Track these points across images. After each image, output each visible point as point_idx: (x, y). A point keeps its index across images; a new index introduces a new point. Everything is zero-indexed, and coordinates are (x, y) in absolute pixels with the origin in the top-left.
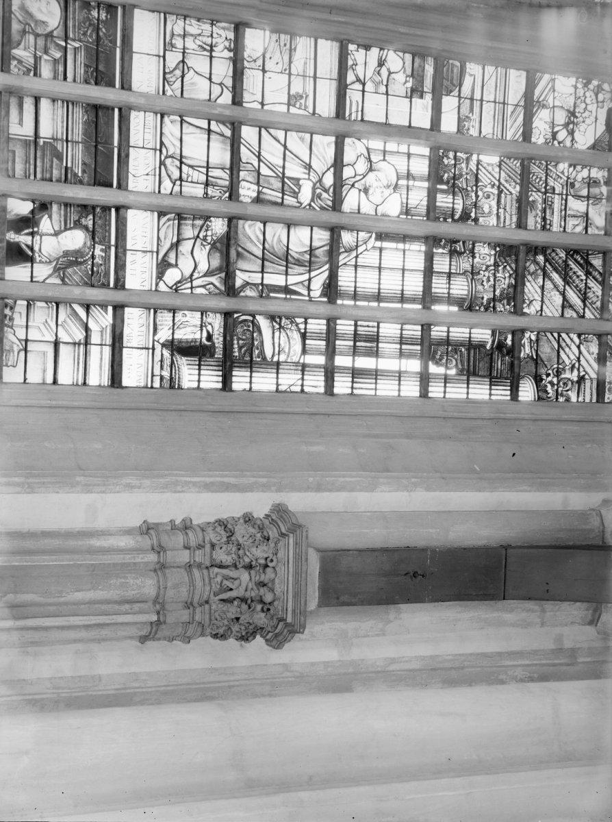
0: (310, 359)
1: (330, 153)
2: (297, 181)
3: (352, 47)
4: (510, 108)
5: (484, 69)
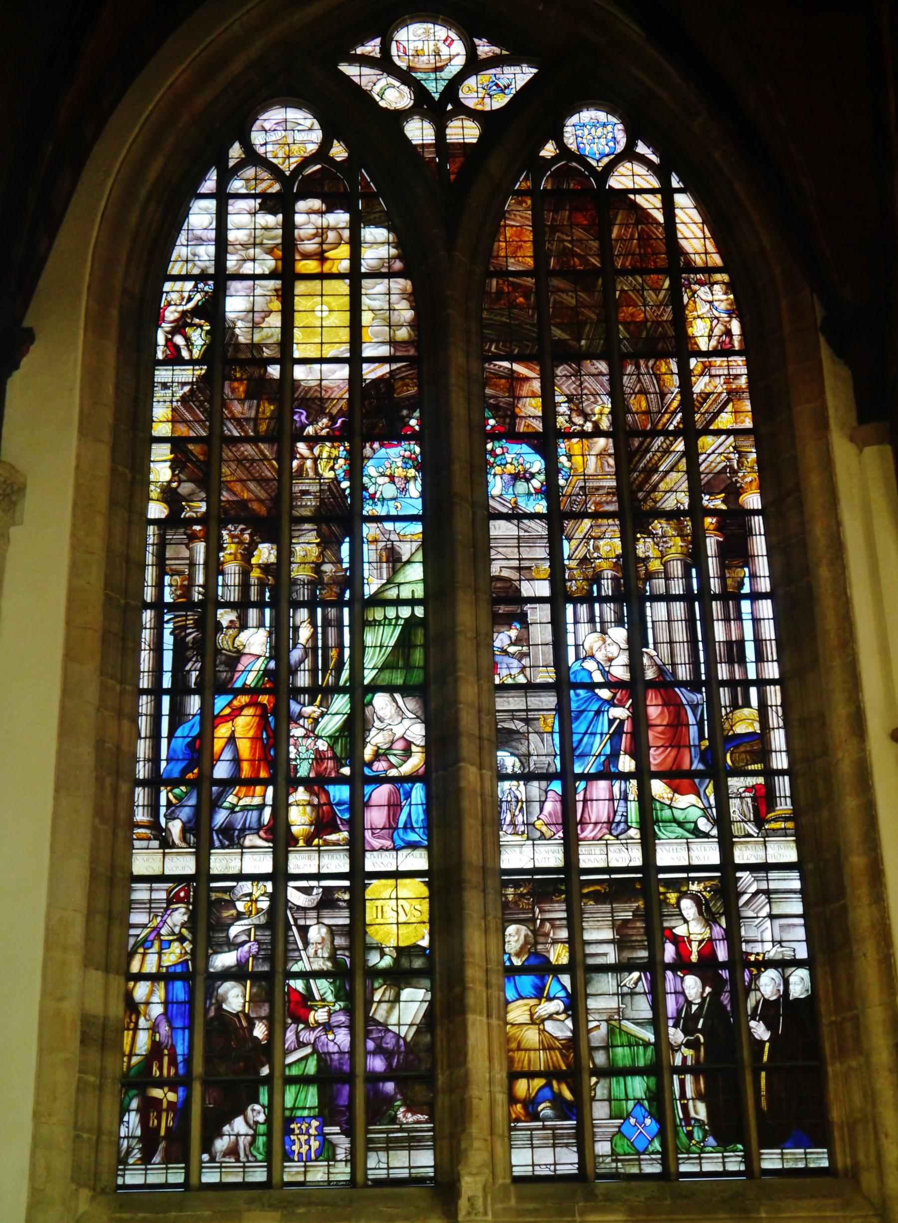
0: (754, 701)
1: (582, 692)
2: (611, 722)
3: (497, 681)
4: (522, 533)
5: (494, 560)
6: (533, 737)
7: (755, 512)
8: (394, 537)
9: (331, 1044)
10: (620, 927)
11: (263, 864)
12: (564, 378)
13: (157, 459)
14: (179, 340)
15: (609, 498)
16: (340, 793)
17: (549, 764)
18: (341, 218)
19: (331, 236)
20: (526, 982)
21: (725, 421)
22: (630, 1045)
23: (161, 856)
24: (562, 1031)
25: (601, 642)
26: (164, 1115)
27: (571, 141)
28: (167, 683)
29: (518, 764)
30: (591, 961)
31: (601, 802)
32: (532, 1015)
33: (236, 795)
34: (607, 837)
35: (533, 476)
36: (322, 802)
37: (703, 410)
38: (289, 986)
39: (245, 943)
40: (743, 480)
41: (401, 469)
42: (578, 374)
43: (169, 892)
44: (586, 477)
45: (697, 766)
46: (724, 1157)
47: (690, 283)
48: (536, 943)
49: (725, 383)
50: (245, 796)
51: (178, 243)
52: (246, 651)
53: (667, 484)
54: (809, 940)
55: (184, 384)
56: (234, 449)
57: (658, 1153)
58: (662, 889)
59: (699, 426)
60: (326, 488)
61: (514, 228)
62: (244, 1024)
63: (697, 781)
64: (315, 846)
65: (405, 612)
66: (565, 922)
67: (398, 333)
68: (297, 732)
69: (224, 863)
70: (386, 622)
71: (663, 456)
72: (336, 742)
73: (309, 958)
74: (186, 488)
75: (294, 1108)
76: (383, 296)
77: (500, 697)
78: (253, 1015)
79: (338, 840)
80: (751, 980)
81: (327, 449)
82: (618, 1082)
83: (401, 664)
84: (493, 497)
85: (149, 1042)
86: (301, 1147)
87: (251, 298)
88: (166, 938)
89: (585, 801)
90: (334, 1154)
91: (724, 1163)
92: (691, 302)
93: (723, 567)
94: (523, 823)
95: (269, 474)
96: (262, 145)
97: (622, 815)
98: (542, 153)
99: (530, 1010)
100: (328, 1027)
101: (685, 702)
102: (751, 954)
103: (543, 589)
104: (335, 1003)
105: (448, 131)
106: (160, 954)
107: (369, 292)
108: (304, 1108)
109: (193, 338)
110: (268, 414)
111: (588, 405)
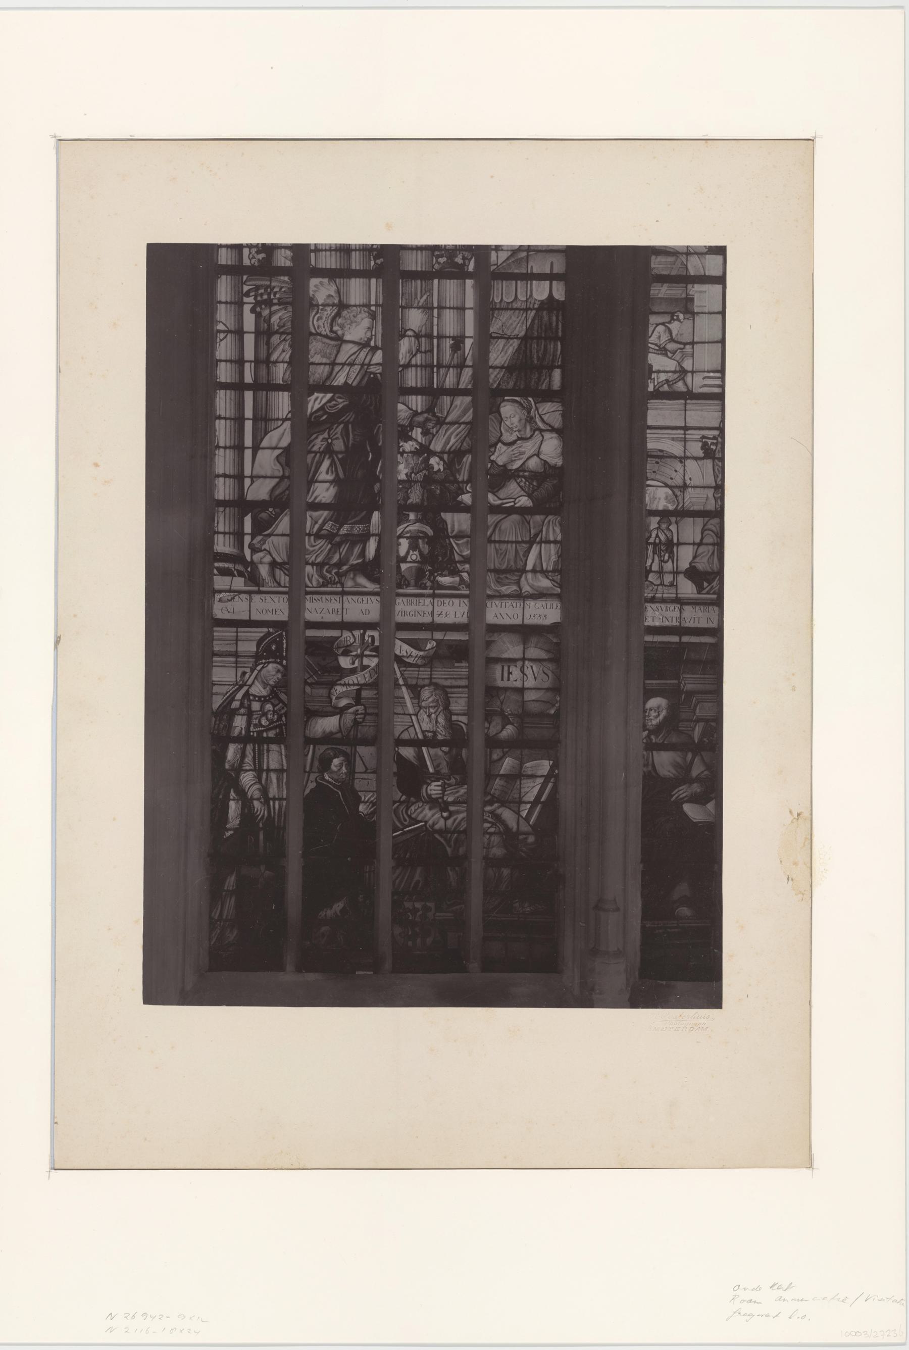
17: (707, 498)
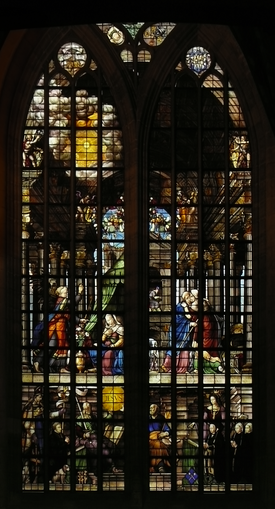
2: (190, 328)
6: (162, 333)
7: (250, 242)
8: (113, 249)
9: (91, 445)
10: (189, 406)
11: (67, 380)
12: (180, 179)
13: (24, 212)
14: (31, 158)
15: (195, 234)
16: (94, 353)
18: (93, 100)
19: (90, 108)
20: (156, 425)
21: (241, 200)
22: (190, 448)
23: (32, 376)
24: (168, 442)
25: (188, 295)
26: (36, 468)
27: (189, 62)
28: (31, 309)
29: (156, 344)
30: (179, 418)
31: (185, 359)
32: (158, 437)
33: (57, 353)
34: (187, 372)
35: (167, 223)
36: (87, 356)
37: (233, 195)
38: (77, 424)
39: (61, 408)
40: (246, 227)
41: (116, 219)
42: (185, 177)
43: (35, 389)
44: (187, 224)
45: (220, 346)
46: (218, 486)
47: (232, 135)
48: (160, 411)
49: (242, 183)
50: (61, 354)
51: (29, 111)
52: (60, 296)
53: (217, 228)
54: (253, 413)
55: (33, 178)
56: (54, 209)
57: (197, 484)
58: (204, 393)
59: (231, 203)
60: (88, 227)
61: (164, 106)
62: (62, 437)
63: (219, 352)
64: (85, 373)
65: (117, 281)
66: (170, 404)
67: (117, 156)
68: (79, 329)
69: (54, 379)
70: (110, 285)
71: (216, 216)
72: (92, 333)
73: (83, 414)
74: (36, 226)
75: (79, 467)
76: (110, 138)
77: (151, 317)
78: (65, 434)
79: (93, 371)
80: (232, 426)
81: (89, 209)
82: (185, 461)
83: (115, 302)
84: (151, 232)
85: (31, 443)
86: (81, 479)
87: (59, 138)
88: (35, 406)
89: (180, 358)
90: (92, 482)
91: (218, 489)
92: (232, 144)
93: (235, 265)
94: (158, 367)
95: (67, 220)
96: (62, 61)
97: (192, 364)
98: (177, 68)
99: (157, 435)
100: (90, 439)
101: (217, 321)
102: (233, 417)
103: (168, 273)
104: (92, 431)
105: (139, 56)
106: (33, 412)
107: (106, 136)
108: (82, 467)
109: (37, 157)
110: (66, 193)
111: (189, 192)
